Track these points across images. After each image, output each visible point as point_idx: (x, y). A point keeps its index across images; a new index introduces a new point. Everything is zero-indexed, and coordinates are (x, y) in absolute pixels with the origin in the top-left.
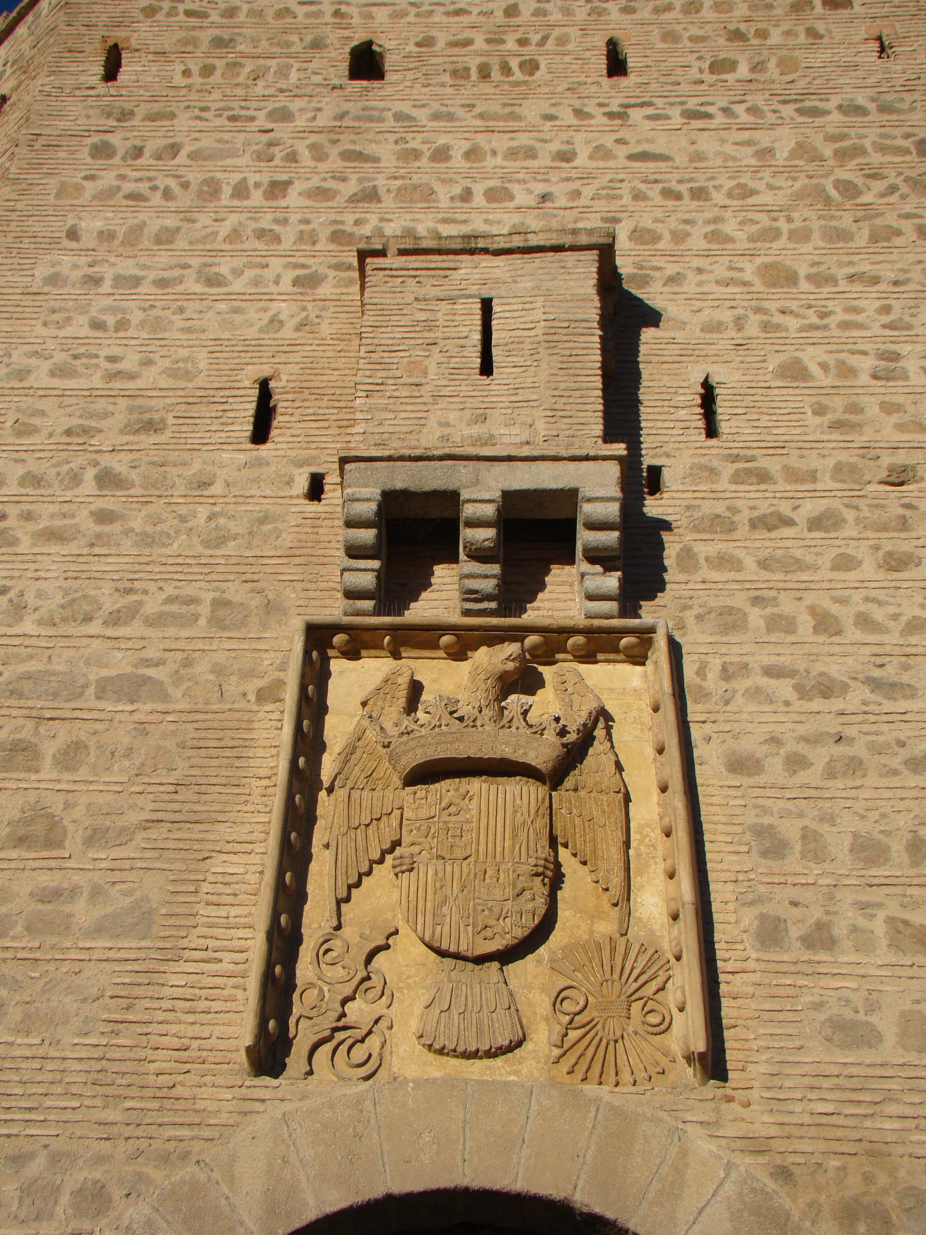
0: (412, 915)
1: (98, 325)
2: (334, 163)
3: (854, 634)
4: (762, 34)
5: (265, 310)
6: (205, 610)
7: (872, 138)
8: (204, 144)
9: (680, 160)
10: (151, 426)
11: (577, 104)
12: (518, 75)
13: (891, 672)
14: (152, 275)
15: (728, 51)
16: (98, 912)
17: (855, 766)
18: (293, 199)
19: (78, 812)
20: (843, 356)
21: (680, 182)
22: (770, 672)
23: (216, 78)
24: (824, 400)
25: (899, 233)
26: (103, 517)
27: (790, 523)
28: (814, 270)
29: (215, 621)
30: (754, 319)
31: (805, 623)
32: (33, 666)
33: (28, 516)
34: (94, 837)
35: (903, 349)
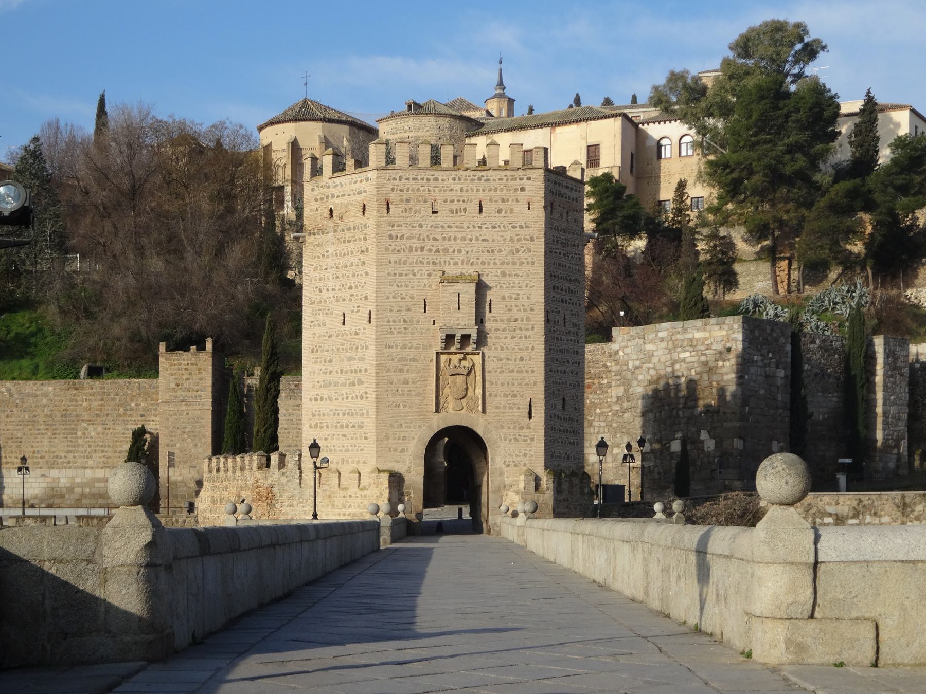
1: (398, 286)
2: (431, 241)
3: (505, 350)
4: (508, 201)
8: (409, 235)
10: (409, 310)
12: (463, 213)
13: (509, 357)
14: (404, 273)
15: (501, 205)
18: (425, 252)
23: (408, 213)
26: (405, 329)
29: (423, 349)
31: (500, 348)
34: (413, 383)
35: (520, 293)
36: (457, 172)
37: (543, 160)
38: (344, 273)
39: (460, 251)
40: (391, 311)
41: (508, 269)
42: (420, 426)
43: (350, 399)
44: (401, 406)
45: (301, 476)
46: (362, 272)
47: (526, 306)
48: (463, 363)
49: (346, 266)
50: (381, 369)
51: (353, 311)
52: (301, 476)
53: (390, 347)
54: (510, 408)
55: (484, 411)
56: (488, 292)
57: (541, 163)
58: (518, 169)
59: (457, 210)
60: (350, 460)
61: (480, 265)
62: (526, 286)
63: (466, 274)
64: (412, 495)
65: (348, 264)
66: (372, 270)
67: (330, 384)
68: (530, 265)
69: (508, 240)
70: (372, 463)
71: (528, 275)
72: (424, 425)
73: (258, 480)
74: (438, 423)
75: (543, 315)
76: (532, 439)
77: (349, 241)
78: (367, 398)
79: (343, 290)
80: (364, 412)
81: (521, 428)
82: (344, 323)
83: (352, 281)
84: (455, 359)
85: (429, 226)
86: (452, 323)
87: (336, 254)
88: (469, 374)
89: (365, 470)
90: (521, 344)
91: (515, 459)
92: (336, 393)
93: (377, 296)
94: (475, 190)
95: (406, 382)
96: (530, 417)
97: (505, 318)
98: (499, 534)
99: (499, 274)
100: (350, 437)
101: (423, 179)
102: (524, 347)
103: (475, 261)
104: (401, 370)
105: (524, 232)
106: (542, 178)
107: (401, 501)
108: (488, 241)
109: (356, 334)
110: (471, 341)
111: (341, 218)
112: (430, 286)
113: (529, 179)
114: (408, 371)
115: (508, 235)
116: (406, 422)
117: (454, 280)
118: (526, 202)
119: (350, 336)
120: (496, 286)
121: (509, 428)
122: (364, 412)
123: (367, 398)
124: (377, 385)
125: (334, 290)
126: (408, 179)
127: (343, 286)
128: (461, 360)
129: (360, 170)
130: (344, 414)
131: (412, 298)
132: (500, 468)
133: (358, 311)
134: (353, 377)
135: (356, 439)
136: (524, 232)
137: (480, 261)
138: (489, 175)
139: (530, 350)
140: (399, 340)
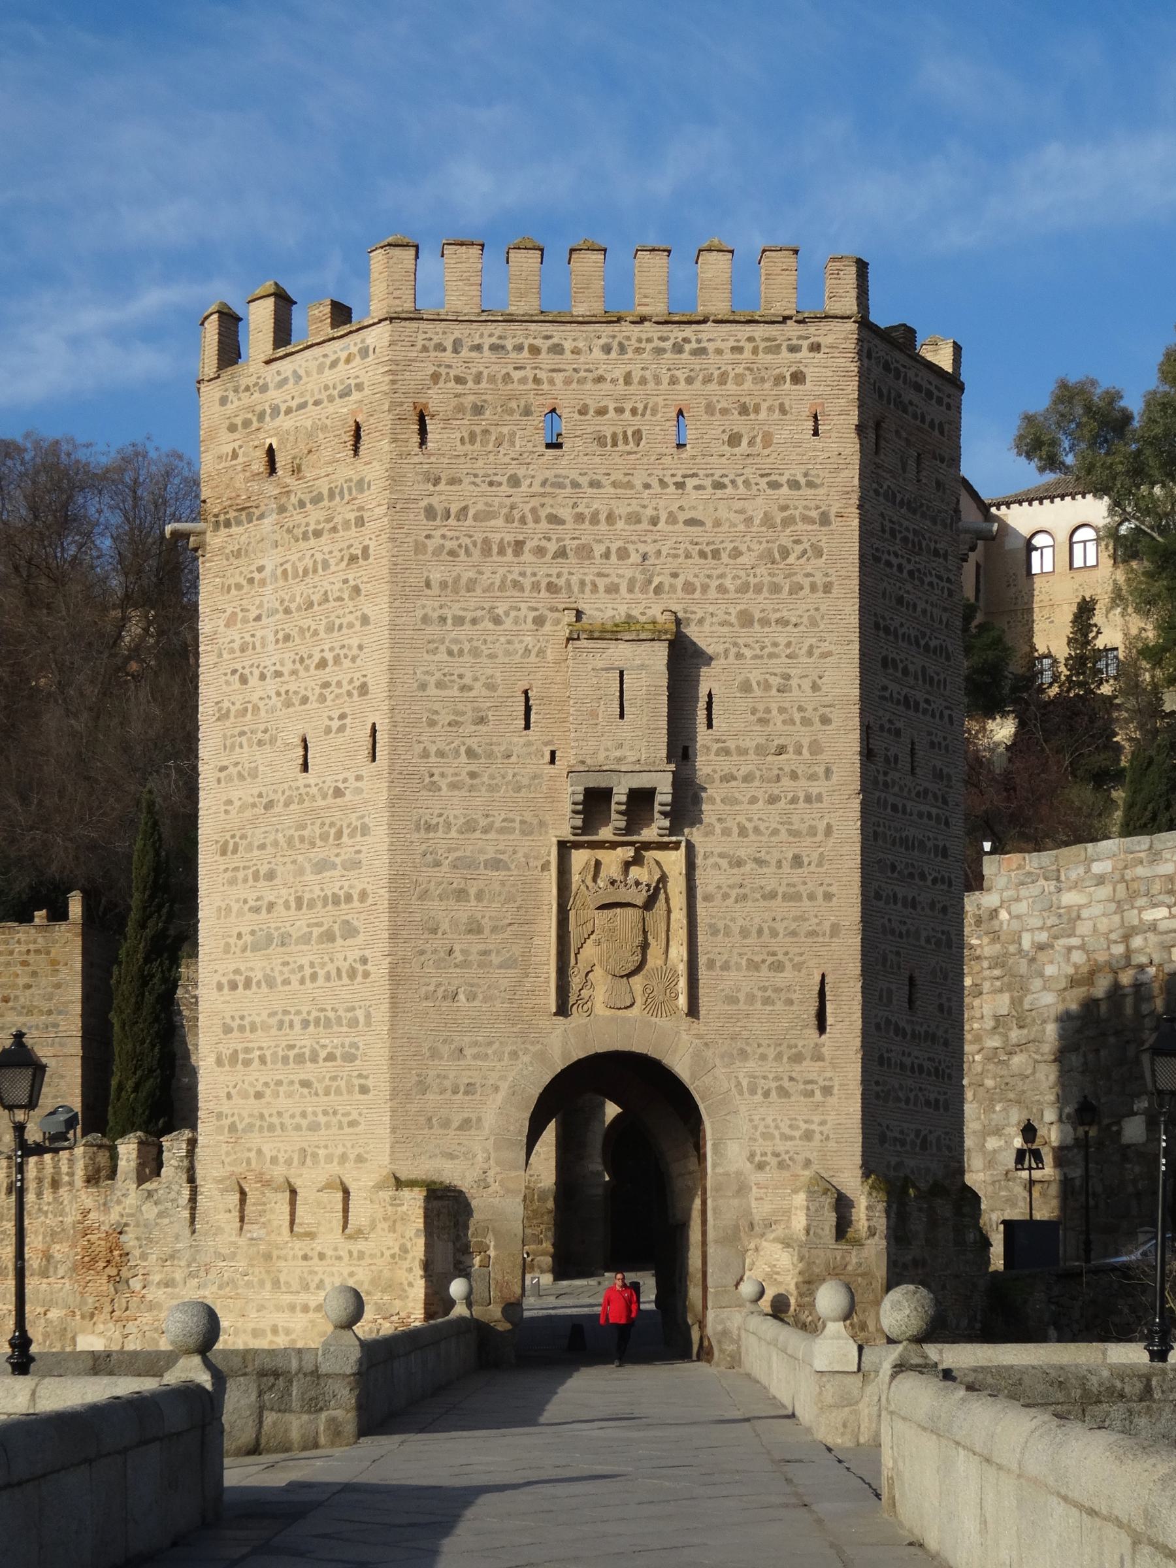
0: (600, 961)
4: (757, 409)
5: (521, 642)
6: (517, 825)
7: (800, 510)
9: (709, 524)
10: (482, 720)
11: (660, 473)
16: (500, 959)
19: (486, 920)
20: (767, 676)
21: (707, 544)
22: (721, 855)
24: (757, 705)
25: (802, 588)
26: (473, 775)
27: (735, 779)
28: (762, 615)
29: (523, 833)
30: (733, 650)
31: (736, 830)
32: (459, 854)
33: (442, 775)
34: (494, 929)
36: (615, 328)
37: (853, 293)
38: (305, 623)
39: (623, 554)
41: (758, 604)
42: (514, 1055)
43: (321, 981)
44: (462, 997)
45: (193, 1200)
46: (351, 618)
47: (810, 708)
48: (635, 872)
49: (311, 605)
51: (328, 730)
52: (193, 1200)
53: (429, 828)
55: (693, 1011)
56: (704, 670)
57: (849, 305)
58: (786, 319)
59: (614, 436)
60: (322, 1152)
61: (680, 593)
62: (810, 653)
63: (642, 619)
64: (492, 1253)
65: (316, 598)
67: (269, 939)
68: (820, 594)
69: (757, 521)
70: (381, 1161)
71: (813, 623)
72: (526, 1052)
73: (86, 1213)
75: (856, 735)
77: (318, 534)
78: (366, 975)
79: (302, 673)
80: (360, 1014)
82: (305, 767)
83: (327, 645)
84: (612, 860)
85: (537, 482)
86: (601, 756)
87: (285, 572)
88: (649, 904)
89: (361, 1182)
90: (795, 819)
91: (781, 1147)
92: (286, 964)
94: (665, 381)
95: (474, 928)
97: (749, 744)
98: (735, 1361)
99: (733, 619)
100: (320, 1088)
102: (804, 828)
103: (667, 580)
104: (461, 895)
105: (801, 502)
106: (851, 345)
107: (463, 1271)
108: (700, 523)
109: (338, 793)
110: (657, 808)
111: (296, 470)
112: (541, 653)
113: (815, 348)
114: (479, 896)
115: (758, 508)
116: (476, 1044)
117: (609, 634)
118: (806, 412)
119: (320, 803)
120: (726, 650)
121: (763, 1057)
122: (360, 1014)
123: (366, 975)
124: (393, 936)
125: (278, 674)
127: (302, 660)
128: (627, 865)
129: (346, 328)
130: (305, 1024)
131: (491, 687)
132: (739, 1173)
133: (342, 729)
134: (328, 917)
135: (338, 1092)
136: (801, 502)
137: (679, 582)
138: (704, 336)
139: (820, 837)
140: (455, 807)
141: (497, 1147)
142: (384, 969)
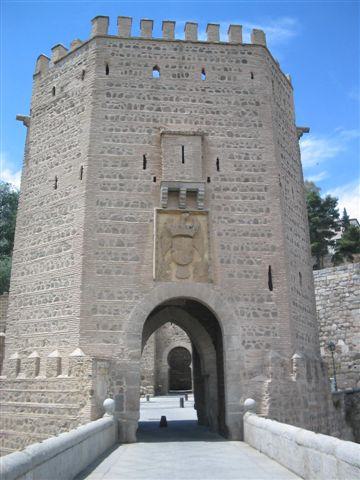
2: (152, 101)
10: (126, 165)
15: (225, 74)
17: (235, 235)
22: (225, 218)
26: (121, 185)
40: (106, 166)
50: (90, 228)
53: (103, 204)
54: (247, 276)
66: (86, 126)
74: (160, 294)
76: (275, 314)
81: (261, 301)
82: (56, 187)
93: (90, 151)
95: (121, 244)
96: (271, 288)
101: (144, 47)
103: (199, 120)
104: (115, 230)
108: (211, 103)
126: (129, 47)
141: (129, 338)
142: (80, 261)
